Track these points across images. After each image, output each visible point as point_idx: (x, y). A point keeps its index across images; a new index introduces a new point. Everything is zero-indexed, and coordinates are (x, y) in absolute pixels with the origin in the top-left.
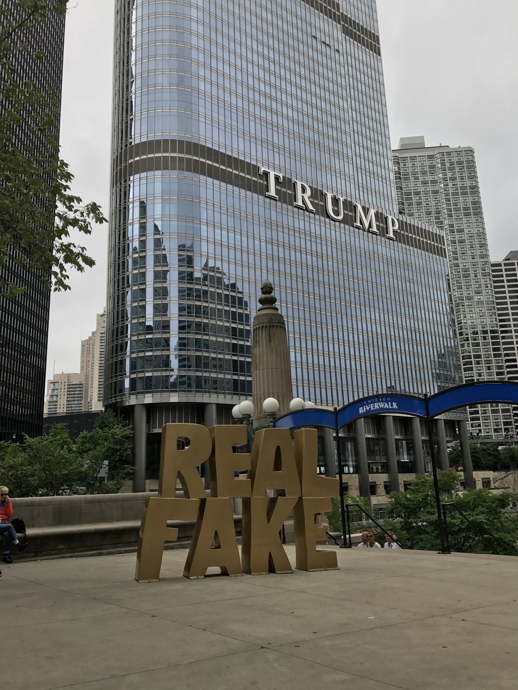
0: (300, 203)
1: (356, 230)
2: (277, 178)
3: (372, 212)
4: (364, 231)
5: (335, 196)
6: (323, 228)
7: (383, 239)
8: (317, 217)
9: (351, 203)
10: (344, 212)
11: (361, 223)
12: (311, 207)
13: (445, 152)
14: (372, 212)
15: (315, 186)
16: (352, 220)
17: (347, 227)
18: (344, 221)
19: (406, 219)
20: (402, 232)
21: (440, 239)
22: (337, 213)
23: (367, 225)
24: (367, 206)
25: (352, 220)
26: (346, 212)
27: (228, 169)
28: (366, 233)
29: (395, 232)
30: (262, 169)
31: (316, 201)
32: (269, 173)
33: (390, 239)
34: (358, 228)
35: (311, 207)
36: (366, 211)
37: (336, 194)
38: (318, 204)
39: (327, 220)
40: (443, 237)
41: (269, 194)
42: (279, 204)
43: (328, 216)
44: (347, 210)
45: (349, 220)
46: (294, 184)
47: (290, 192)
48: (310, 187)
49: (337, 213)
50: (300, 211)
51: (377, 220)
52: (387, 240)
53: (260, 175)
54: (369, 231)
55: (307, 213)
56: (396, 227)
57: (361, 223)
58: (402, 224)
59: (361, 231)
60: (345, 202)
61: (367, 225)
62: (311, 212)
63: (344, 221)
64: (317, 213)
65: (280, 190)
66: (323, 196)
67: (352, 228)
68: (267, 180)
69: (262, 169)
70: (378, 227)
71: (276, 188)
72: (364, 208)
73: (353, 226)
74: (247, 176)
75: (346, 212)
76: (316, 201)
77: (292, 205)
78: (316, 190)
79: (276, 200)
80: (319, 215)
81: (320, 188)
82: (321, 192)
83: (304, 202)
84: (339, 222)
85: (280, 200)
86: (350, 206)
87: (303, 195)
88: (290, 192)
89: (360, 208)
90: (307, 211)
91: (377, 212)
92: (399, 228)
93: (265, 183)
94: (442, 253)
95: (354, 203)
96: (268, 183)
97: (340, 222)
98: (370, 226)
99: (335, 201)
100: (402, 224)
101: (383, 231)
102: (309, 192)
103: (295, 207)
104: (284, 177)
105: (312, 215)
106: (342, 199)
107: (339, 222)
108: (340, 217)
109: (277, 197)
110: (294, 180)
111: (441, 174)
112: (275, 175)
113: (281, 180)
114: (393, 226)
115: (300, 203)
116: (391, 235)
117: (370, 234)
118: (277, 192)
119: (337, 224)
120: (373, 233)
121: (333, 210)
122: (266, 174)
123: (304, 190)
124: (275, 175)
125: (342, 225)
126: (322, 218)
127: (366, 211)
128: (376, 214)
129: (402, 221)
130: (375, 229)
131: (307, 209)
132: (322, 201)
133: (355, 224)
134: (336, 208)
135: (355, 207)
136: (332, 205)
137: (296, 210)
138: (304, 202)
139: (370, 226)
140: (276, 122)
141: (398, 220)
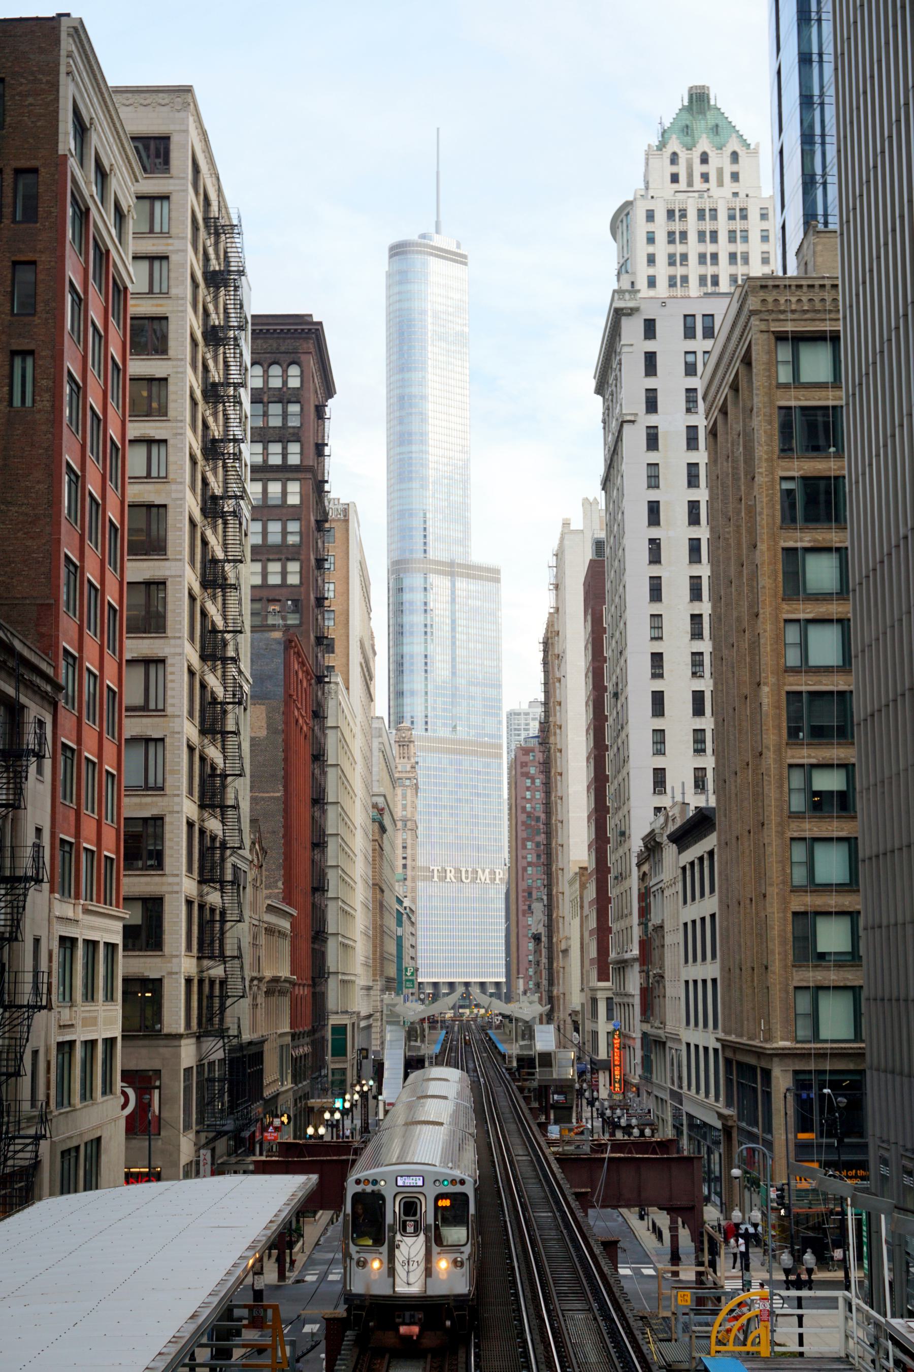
3: (487, 871)
12: (454, 880)
14: (487, 871)
30: (432, 868)
35: (454, 880)
36: (484, 871)
43: (462, 881)
49: (467, 878)
56: (501, 876)
69: (432, 868)
70: (491, 879)
89: (480, 872)
99: (467, 871)
102: (453, 871)
108: (469, 881)
118: (439, 877)
127: (484, 871)
130: (488, 881)
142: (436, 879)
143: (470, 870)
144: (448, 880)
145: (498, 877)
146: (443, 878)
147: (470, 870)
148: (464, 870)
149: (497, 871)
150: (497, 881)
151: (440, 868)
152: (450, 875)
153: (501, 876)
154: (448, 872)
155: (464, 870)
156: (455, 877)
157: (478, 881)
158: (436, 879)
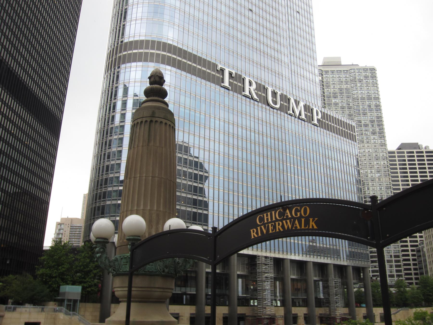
0: (247, 93)
1: (289, 116)
2: (230, 74)
3: (302, 104)
4: (296, 117)
5: (274, 91)
6: (264, 113)
7: (309, 124)
8: (260, 104)
9: (286, 96)
13: (356, 69)
14: (302, 104)
15: (259, 82)
16: (286, 109)
17: (282, 113)
18: (281, 109)
19: (326, 111)
20: (324, 121)
21: (351, 128)
22: (275, 103)
24: (298, 99)
25: (286, 109)
26: (282, 103)
27: (194, 65)
28: (296, 119)
29: (318, 120)
31: (260, 93)
32: (225, 69)
33: (314, 125)
34: (290, 115)
35: (255, 97)
37: (275, 89)
38: (261, 95)
39: (268, 107)
40: (354, 127)
41: (224, 84)
42: (231, 92)
43: (268, 105)
44: (283, 101)
45: (284, 109)
46: (243, 79)
47: (240, 85)
48: (255, 82)
49: (275, 103)
50: (247, 99)
51: (305, 110)
52: (313, 126)
53: (217, 70)
54: (299, 118)
55: (252, 101)
56: (320, 117)
58: (323, 114)
59: (293, 118)
60: (281, 95)
61: (297, 114)
63: (281, 109)
65: (232, 83)
66: (265, 90)
67: (286, 115)
68: (223, 75)
70: (306, 115)
71: (229, 82)
72: (295, 101)
73: (287, 113)
74: (208, 71)
75: (282, 103)
76: (260, 93)
77: (241, 94)
78: (260, 85)
79: (229, 90)
80: (261, 103)
81: (263, 83)
82: (264, 87)
84: (277, 109)
85: (232, 90)
87: (250, 87)
88: (240, 85)
89: (292, 101)
90: (253, 99)
91: (306, 105)
92: (322, 118)
93: (221, 77)
94: (352, 138)
95: (289, 97)
96: (223, 77)
98: (300, 114)
99: (274, 94)
100: (323, 114)
101: (310, 119)
102: (254, 86)
103: (243, 96)
104: (236, 74)
105: (256, 103)
106: (279, 93)
107: (277, 109)
108: (278, 106)
109: (230, 87)
110: (243, 76)
111: (353, 84)
112: (229, 71)
113: (234, 75)
114: (317, 115)
115: (247, 93)
116: (315, 122)
117: (300, 121)
118: (230, 83)
119: (275, 111)
120: (302, 120)
121: (272, 100)
122: (222, 70)
124: (229, 71)
125: (279, 112)
126: (264, 106)
128: (305, 106)
129: (324, 113)
130: (303, 117)
131: (252, 98)
132: (264, 93)
133: (288, 112)
134: (274, 99)
135: (289, 100)
136: (272, 97)
137: (244, 98)
138: (250, 93)
139: (300, 114)
140: (232, 34)
141: (321, 112)
142: (226, 84)
156: (257, 94)
158: (226, 84)
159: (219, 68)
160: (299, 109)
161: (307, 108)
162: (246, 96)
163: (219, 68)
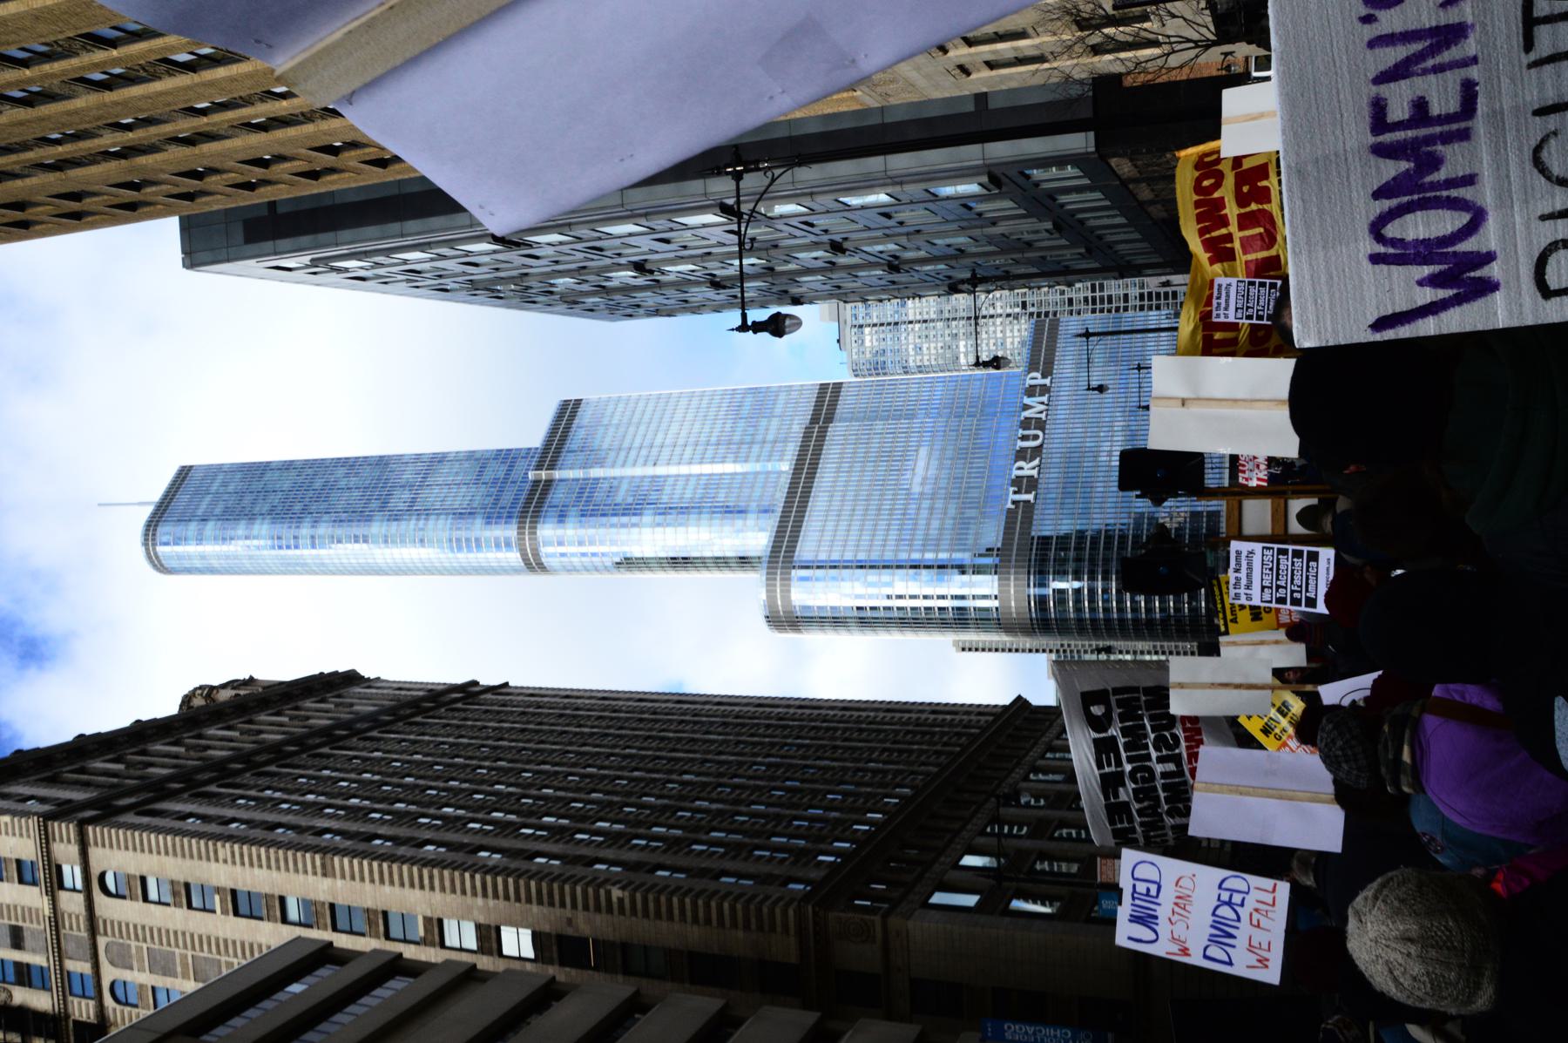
2: (1015, 493)
3: (1027, 401)
8: (1044, 456)
9: (1022, 422)
10: (1035, 429)
11: (1041, 412)
12: (1036, 462)
14: (1027, 401)
17: (1047, 427)
23: (1042, 407)
29: (1044, 376)
30: (1010, 506)
36: (1026, 407)
39: (1045, 446)
48: (1016, 462)
49: (1036, 437)
51: (1034, 396)
56: (1038, 375)
57: (1041, 412)
61: (1042, 407)
62: (1040, 461)
63: (1043, 430)
64: (1040, 456)
66: (1023, 450)
68: (1019, 502)
69: (1010, 506)
77: (1037, 480)
83: (1034, 468)
86: (1026, 423)
89: (1027, 414)
97: (1044, 434)
98: (1043, 403)
99: (1024, 438)
101: (1044, 390)
102: (1021, 464)
105: (1043, 461)
108: (1040, 433)
113: (1016, 489)
116: (1047, 381)
118: (1028, 492)
122: (1014, 502)
123: (1020, 468)
125: (1047, 431)
126: (1044, 451)
127: (1026, 407)
130: (1045, 399)
135: (1026, 418)
138: (1034, 468)
139: (1043, 403)
142: (1030, 497)
143: (1021, 432)
144: (1034, 473)
145: (1041, 381)
146: (1031, 484)
147: (1021, 432)
148: (1021, 444)
149: (1029, 382)
150: (1047, 381)
151: (1012, 489)
152: (1028, 469)
153: (1038, 375)
154: (1020, 473)
155: (1021, 444)
157: (1043, 416)
158: (1030, 497)
159: (1013, 507)
160: (1036, 406)
161: (1031, 391)
162: (1039, 473)
163: (1013, 507)
